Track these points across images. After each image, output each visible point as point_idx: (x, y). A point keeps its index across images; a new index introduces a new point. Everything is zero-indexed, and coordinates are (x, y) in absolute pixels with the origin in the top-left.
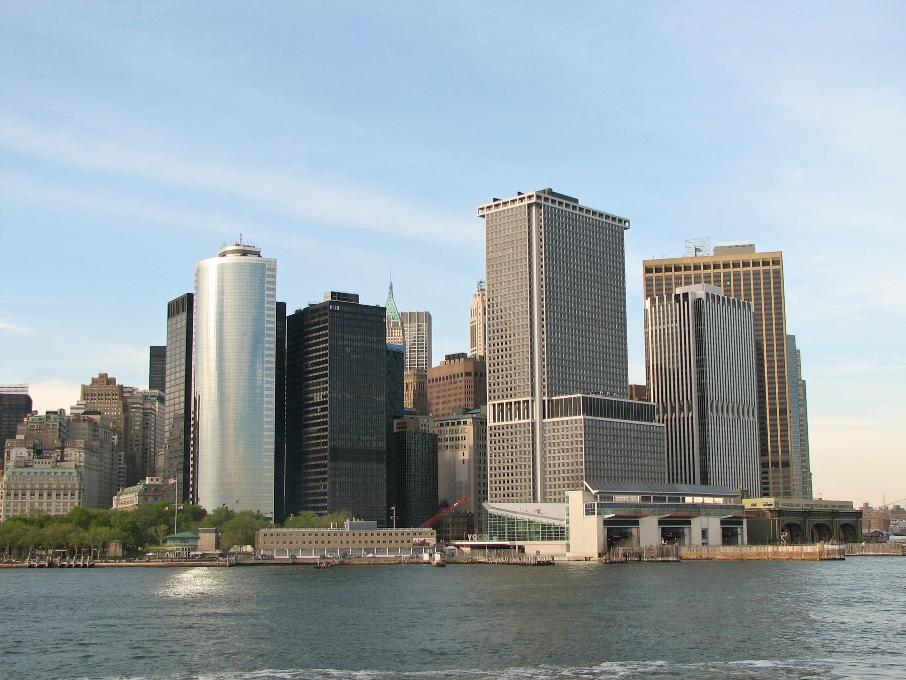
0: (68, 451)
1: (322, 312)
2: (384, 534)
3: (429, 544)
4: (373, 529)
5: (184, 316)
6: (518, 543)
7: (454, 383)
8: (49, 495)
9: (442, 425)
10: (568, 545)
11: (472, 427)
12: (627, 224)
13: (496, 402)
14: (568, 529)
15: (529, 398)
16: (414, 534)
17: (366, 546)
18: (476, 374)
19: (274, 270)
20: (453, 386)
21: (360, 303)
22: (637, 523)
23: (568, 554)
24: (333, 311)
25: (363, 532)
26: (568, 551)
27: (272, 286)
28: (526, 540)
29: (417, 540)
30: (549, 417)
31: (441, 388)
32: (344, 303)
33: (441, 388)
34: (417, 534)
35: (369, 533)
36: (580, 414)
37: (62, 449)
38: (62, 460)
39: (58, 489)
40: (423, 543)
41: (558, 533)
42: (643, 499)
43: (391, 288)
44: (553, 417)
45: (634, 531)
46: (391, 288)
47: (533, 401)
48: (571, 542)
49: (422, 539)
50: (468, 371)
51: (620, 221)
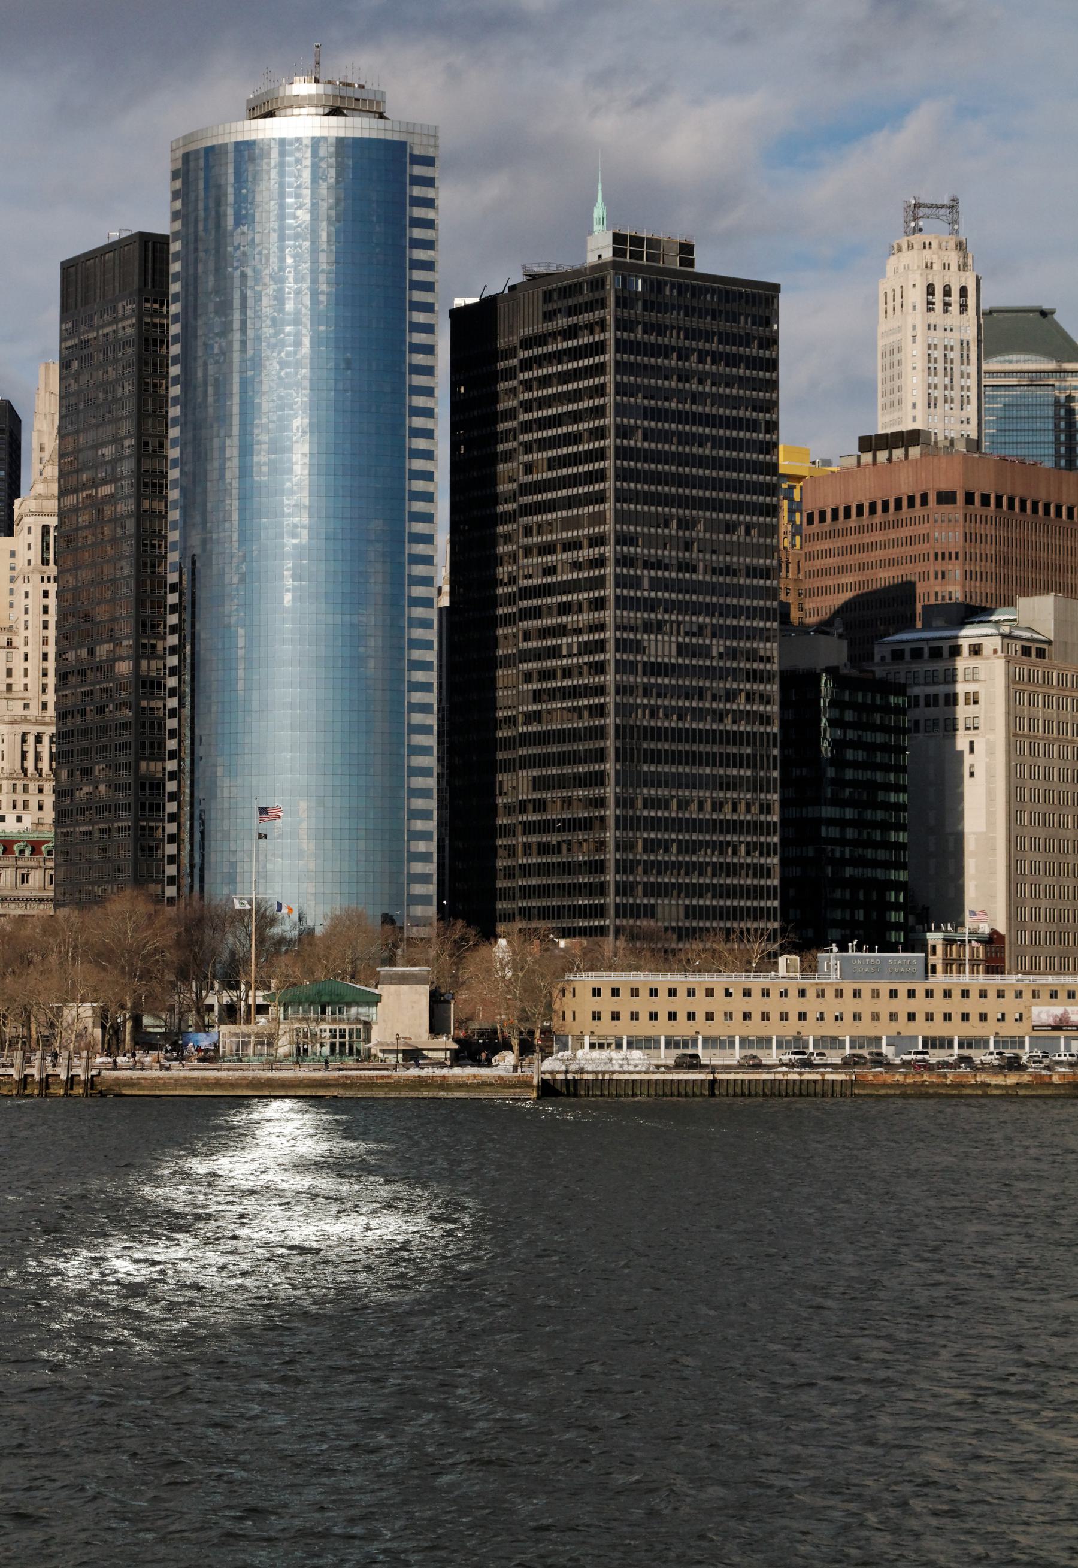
1: (586, 295)
2: (947, 994)
4: (912, 976)
5: (982, 308)
7: (898, 524)
11: (998, 667)
16: (1035, 995)
17: (893, 1028)
18: (969, 498)
20: (893, 534)
21: (700, 267)
31: (853, 540)
33: (853, 540)
34: (1045, 995)
35: (902, 989)
50: (944, 487)
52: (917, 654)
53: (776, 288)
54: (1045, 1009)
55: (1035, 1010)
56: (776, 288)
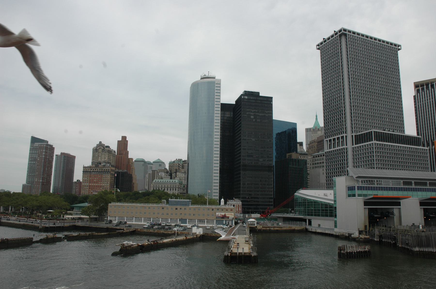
0: (178, 173)
3: (228, 217)
6: (308, 217)
8: (173, 189)
9: (314, 157)
10: (336, 223)
12: (400, 47)
13: (328, 139)
14: (335, 208)
15: (344, 135)
19: (220, 84)
22: (399, 204)
23: (336, 230)
24: (244, 99)
25: (179, 207)
26: (336, 226)
27: (218, 91)
28: (312, 215)
29: (219, 214)
30: (356, 144)
32: (246, 93)
36: (372, 140)
37: (176, 172)
38: (176, 177)
39: (170, 187)
40: (224, 217)
41: (329, 211)
42: (405, 183)
43: (316, 116)
44: (358, 144)
45: (396, 212)
46: (316, 116)
47: (346, 136)
48: (338, 219)
49: (223, 214)
51: (395, 45)
52: (316, 157)
53: (272, 98)
54: (220, 213)
55: (217, 214)
56: (272, 98)
